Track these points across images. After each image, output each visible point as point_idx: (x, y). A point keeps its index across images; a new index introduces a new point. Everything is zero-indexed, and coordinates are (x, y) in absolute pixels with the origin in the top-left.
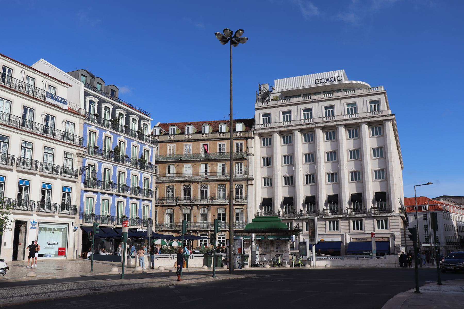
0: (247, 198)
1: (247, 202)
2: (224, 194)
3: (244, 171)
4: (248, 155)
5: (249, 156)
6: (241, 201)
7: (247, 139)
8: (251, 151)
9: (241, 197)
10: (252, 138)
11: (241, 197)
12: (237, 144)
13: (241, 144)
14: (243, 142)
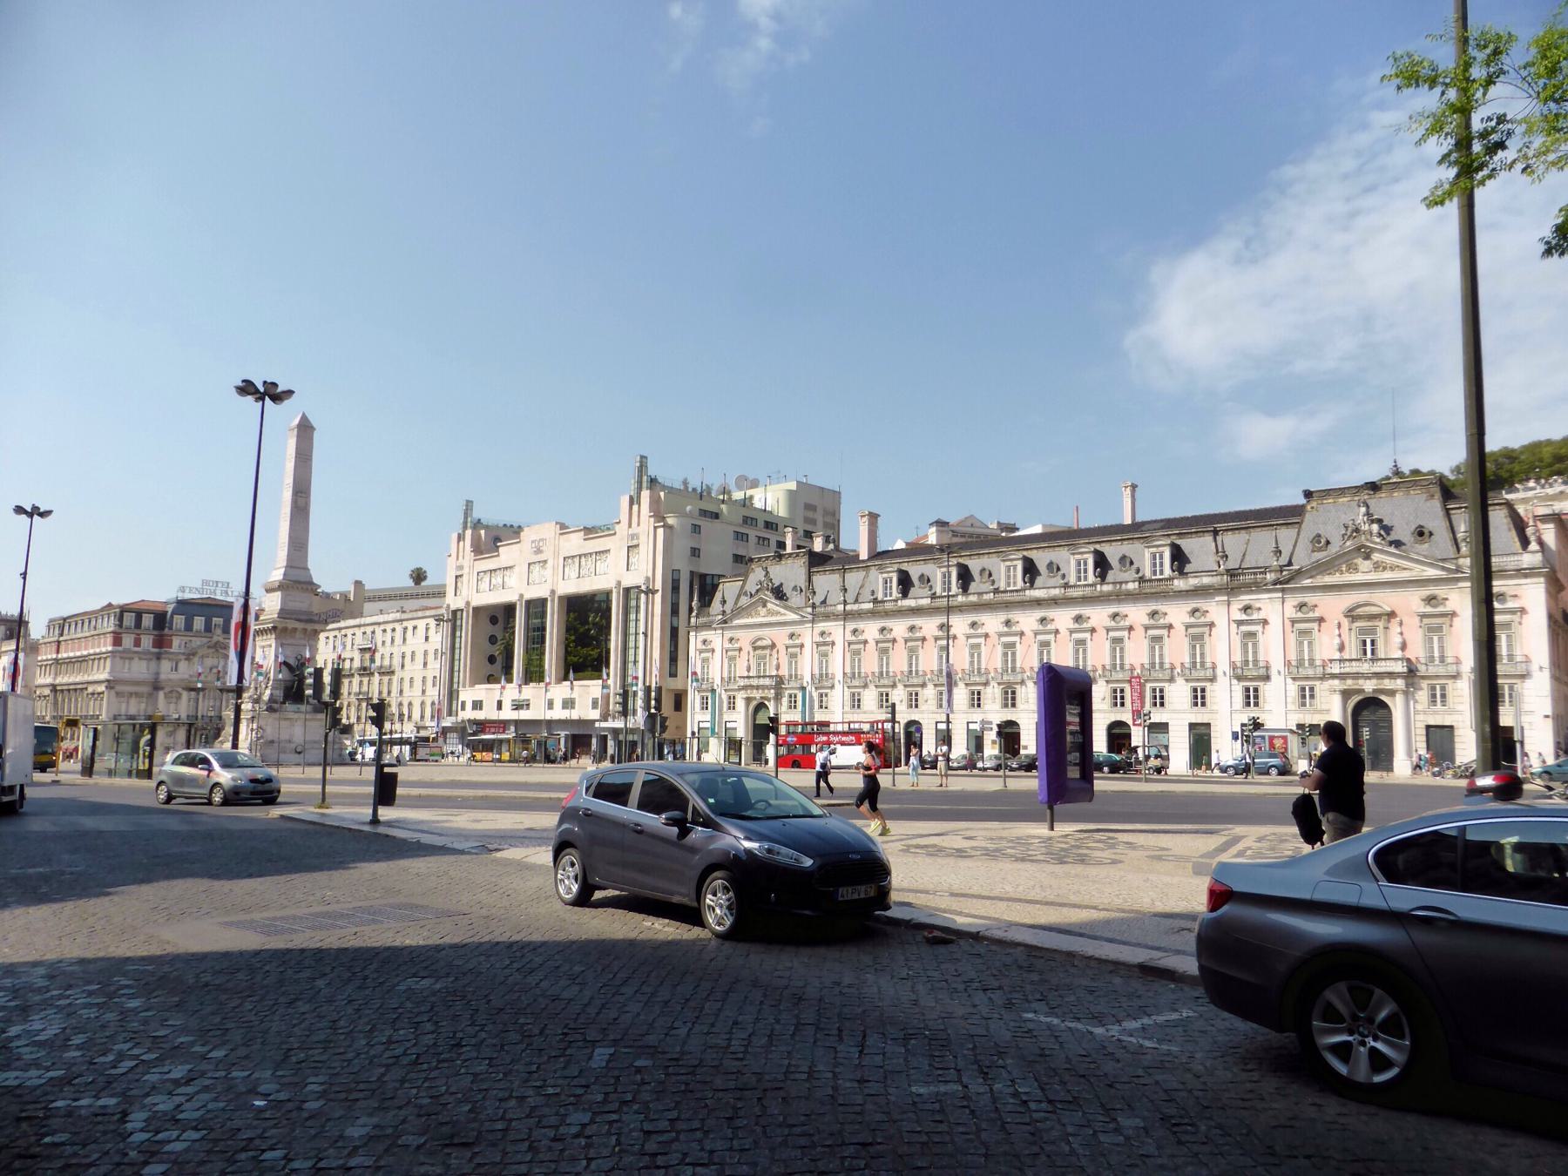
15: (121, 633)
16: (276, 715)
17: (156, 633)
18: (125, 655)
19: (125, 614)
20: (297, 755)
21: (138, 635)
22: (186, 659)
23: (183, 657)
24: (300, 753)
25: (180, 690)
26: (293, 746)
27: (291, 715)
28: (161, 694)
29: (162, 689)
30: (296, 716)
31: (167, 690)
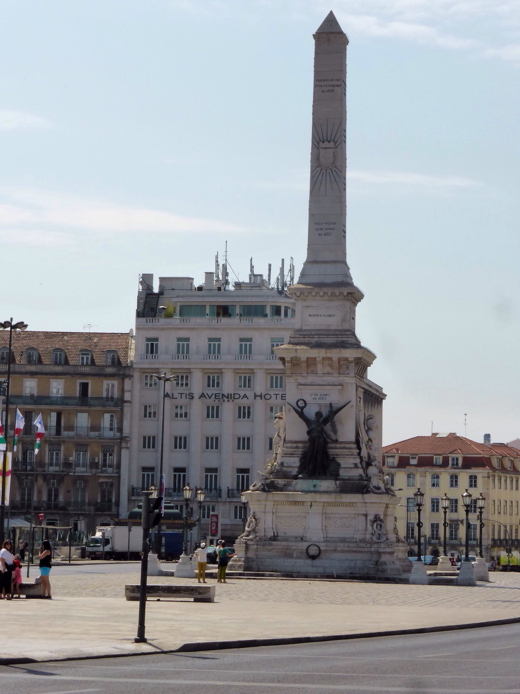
0: (119, 466)
1: (119, 473)
2: (84, 459)
3: (116, 427)
4: (124, 402)
5: (125, 404)
6: (110, 470)
8: (127, 396)
10: (131, 377)
12: (108, 385)
13: (113, 386)
14: (116, 383)
16: (278, 496)
20: (309, 562)
24: (313, 558)
26: (304, 546)
27: (300, 496)
30: (308, 498)
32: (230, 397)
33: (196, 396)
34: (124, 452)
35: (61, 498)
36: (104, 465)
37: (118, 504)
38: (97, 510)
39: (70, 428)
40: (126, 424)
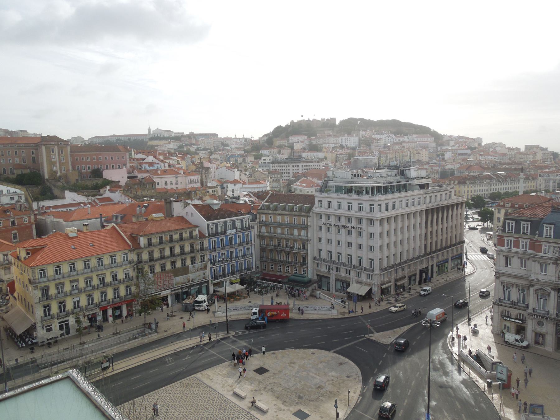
0: (307, 250)
1: (307, 252)
7: (308, 217)
8: (309, 224)
9: (305, 249)
11: (305, 249)
14: (305, 218)
15: (503, 236)
17: (531, 237)
18: (505, 254)
19: (507, 221)
21: (516, 238)
22: (553, 263)
23: (550, 261)
25: (548, 289)
28: (532, 289)
29: (533, 286)
31: (537, 287)
32: (344, 227)
33: (333, 225)
34: (309, 245)
35: (290, 260)
36: (303, 249)
37: (307, 263)
38: (301, 265)
39: (291, 234)
40: (309, 234)
